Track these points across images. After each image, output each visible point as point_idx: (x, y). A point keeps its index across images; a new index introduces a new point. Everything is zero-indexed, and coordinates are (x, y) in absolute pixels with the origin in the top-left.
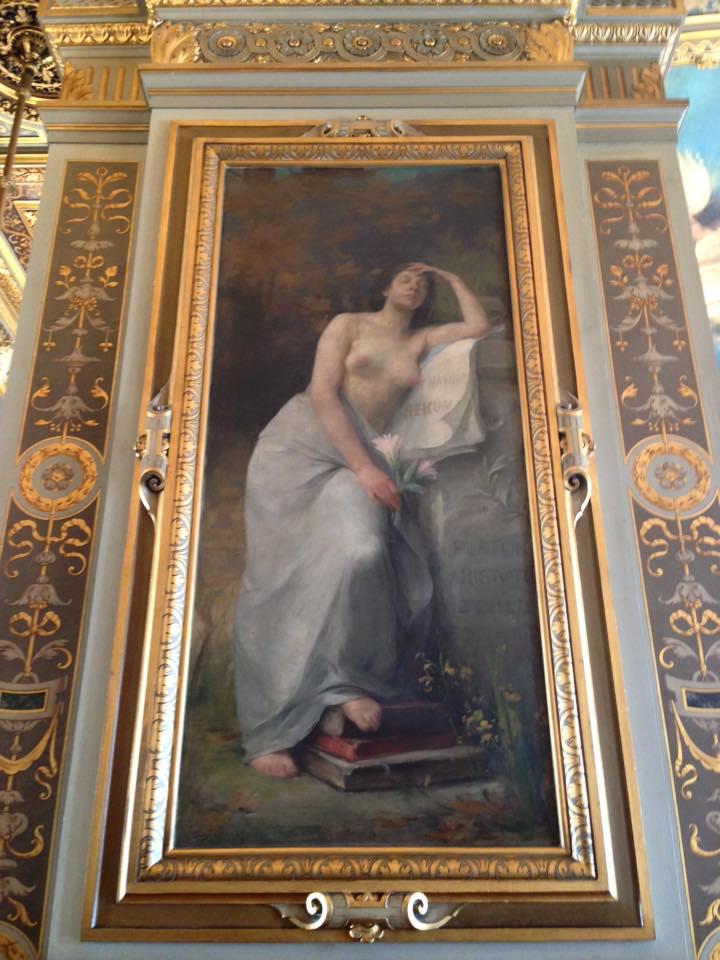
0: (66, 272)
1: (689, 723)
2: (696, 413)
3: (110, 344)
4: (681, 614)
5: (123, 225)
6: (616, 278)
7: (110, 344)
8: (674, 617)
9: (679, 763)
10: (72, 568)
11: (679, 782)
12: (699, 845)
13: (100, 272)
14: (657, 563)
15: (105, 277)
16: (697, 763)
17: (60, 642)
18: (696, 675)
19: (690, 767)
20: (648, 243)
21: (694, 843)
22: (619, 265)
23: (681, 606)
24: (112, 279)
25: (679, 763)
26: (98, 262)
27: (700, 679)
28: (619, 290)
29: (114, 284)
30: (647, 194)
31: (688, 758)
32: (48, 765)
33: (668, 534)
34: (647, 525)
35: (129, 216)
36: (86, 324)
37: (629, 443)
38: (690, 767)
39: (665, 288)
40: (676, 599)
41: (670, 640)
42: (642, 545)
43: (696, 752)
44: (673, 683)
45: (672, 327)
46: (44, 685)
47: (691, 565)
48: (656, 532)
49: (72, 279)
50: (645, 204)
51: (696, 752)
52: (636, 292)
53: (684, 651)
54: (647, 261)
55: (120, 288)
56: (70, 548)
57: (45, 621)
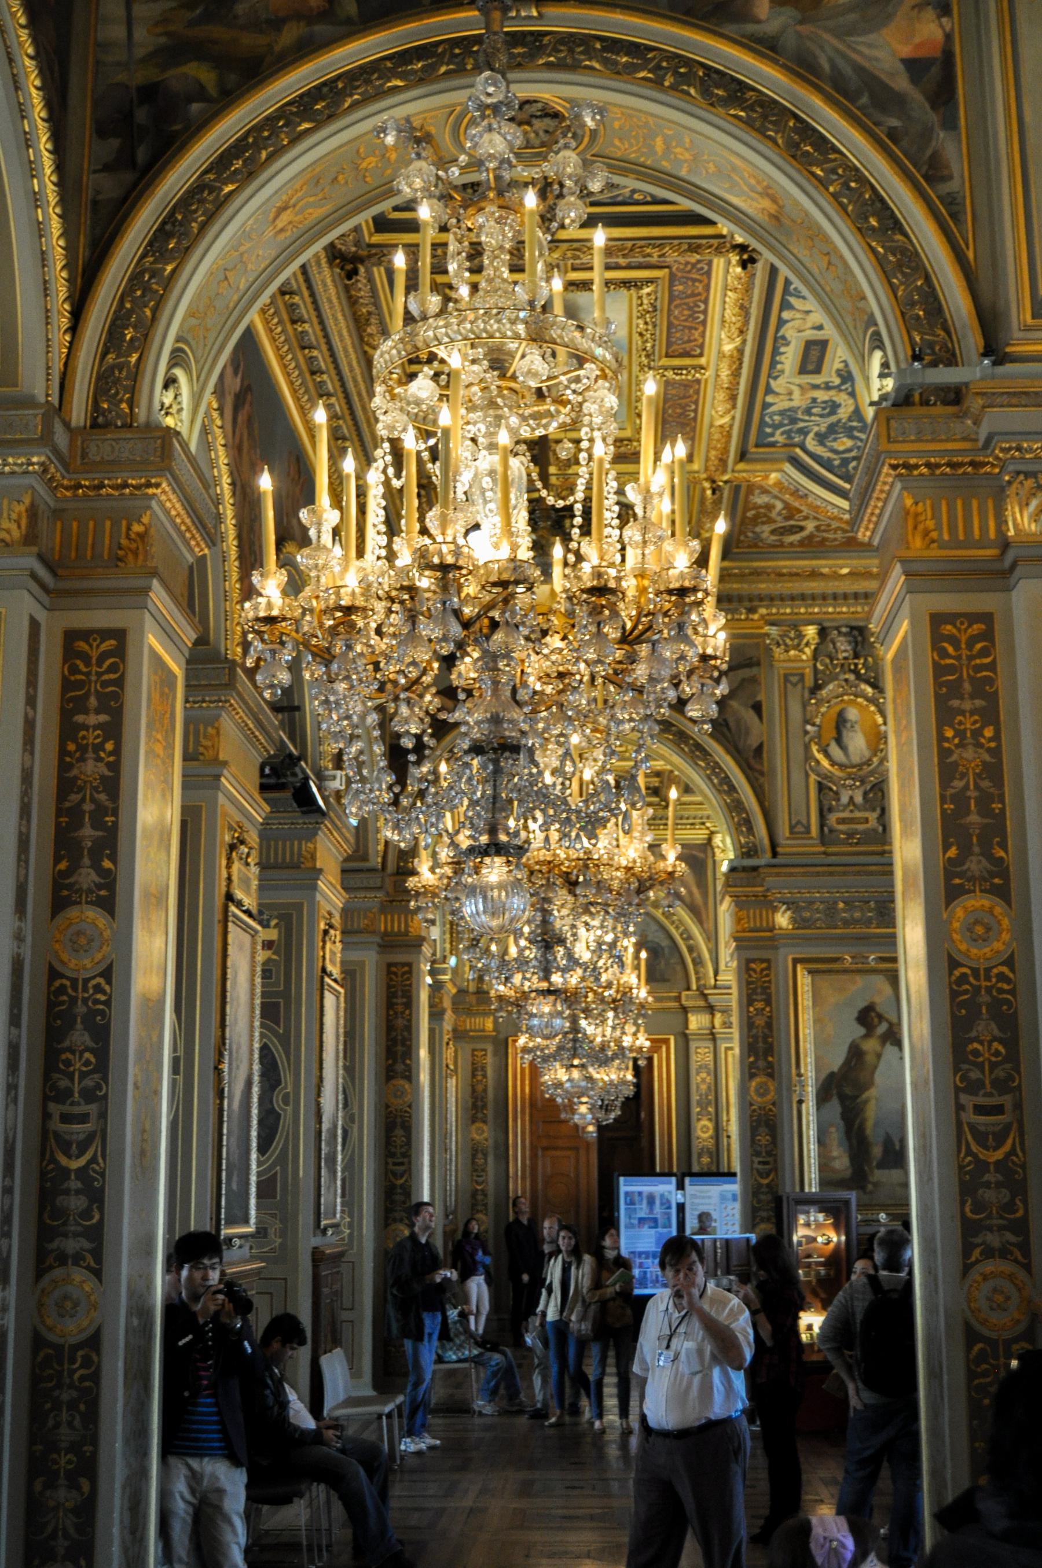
1: (972, 1127)
2: (1005, 874)
4: (976, 1045)
6: (947, 740)
8: (970, 1047)
9: (962, 1155)
11: (961, 1168)
12: (971, 1211)
14: (962, 1004)
16: (975, 1156)
18: (982, 1092)
19: (969, 1158)
20: (979, 703)
21: (967, 1209)
22: (952, 726)
23: (976, 1039)
25: (962, 1155)
27: (985, 1095)
28: (949, 752)
30: (982, 648)
31: (969, 1152)
33: (972, 980)
34: (957, 973)
37: (948, 902)
38: (969, 1158)
39: (989, 750)
40: (973, 1034)
41: (965, 1066)
42: (951, 989)
43: (974, 1148)
44: (964, 1098)
45: (992, 790)
46: (89, 1107)
47: (988, 1006)
48: (963, 979)
50: (978, 661)
51: (974, 1148)
52: (965, 755)
53: (975, 1075)
54: (975, 722)
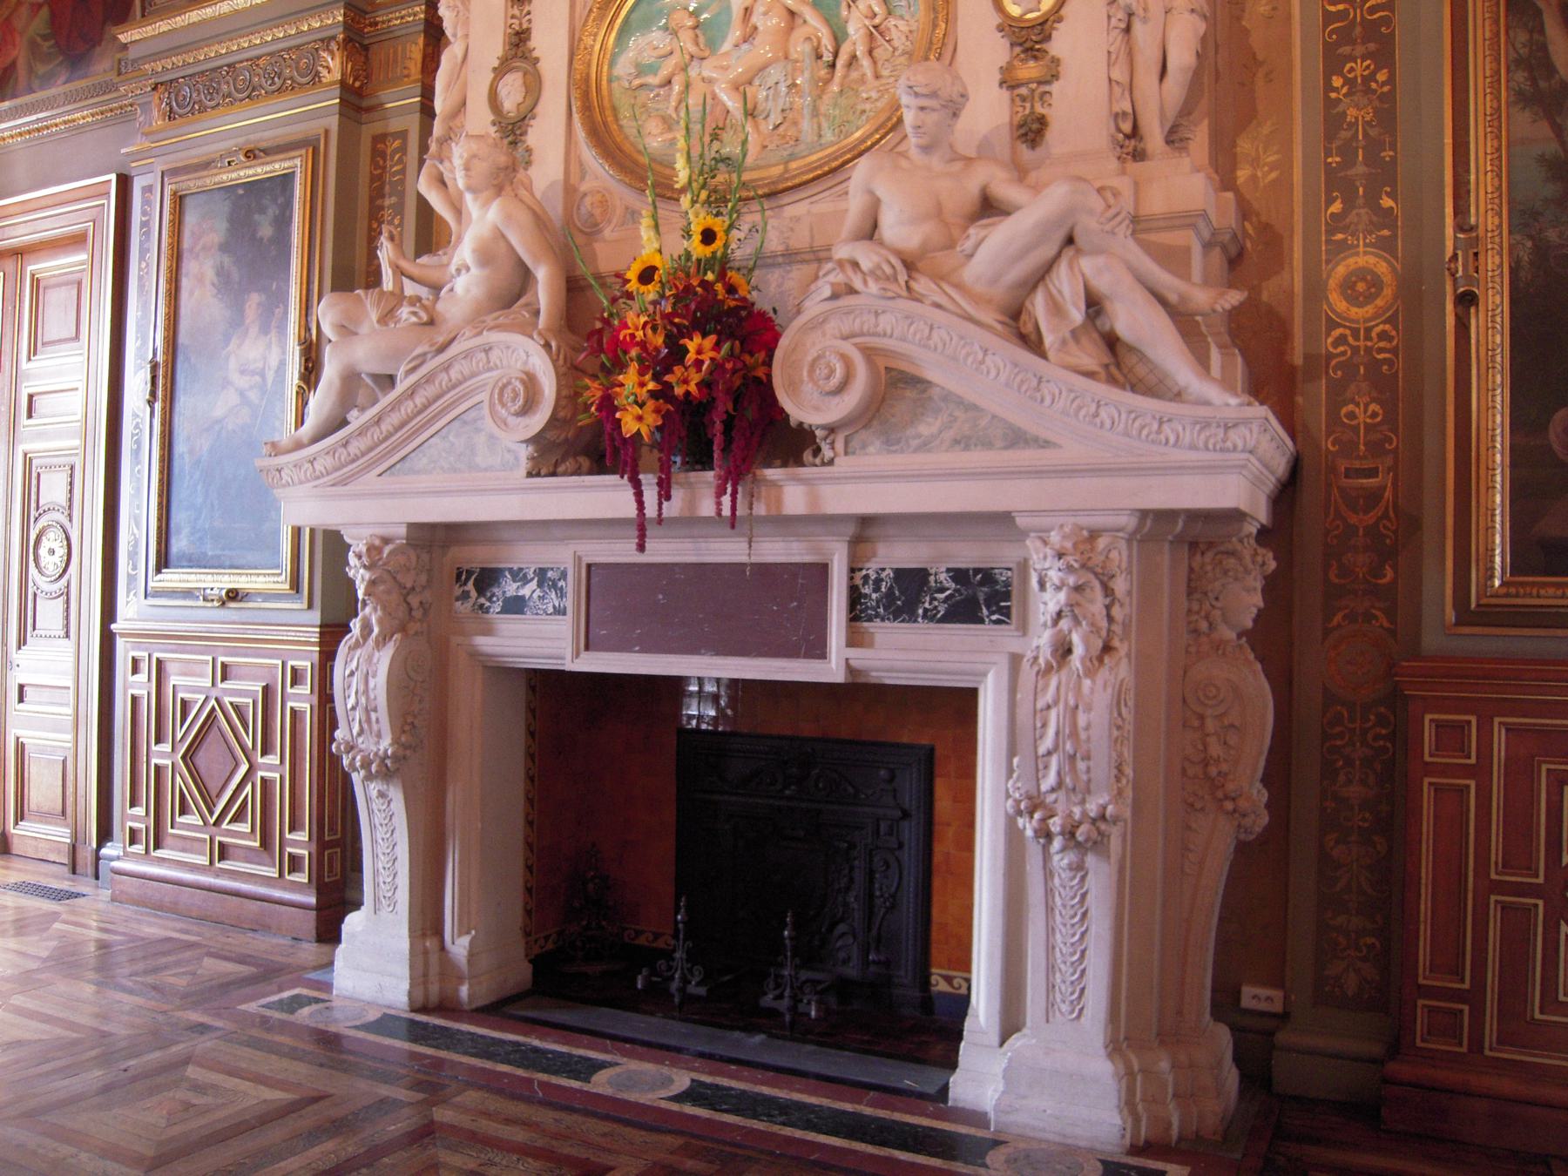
0: (1337, 82)
3: (1391, 153)
5: (1387, 21)
7: (1391, 153)
10: (1385, 367)
13: (1372, 77)
15: (1376, 82)
17: (1385, 427)
24: (1384, 84)
26: (1368, 67)
29: (1386, 89)
32: (1390, 520)
35: (1393, 11)
36: (1366, 134)
49: (1345, 90)
55: (1393, 91)
56: (1381, 350)
57: (1369, 413)
